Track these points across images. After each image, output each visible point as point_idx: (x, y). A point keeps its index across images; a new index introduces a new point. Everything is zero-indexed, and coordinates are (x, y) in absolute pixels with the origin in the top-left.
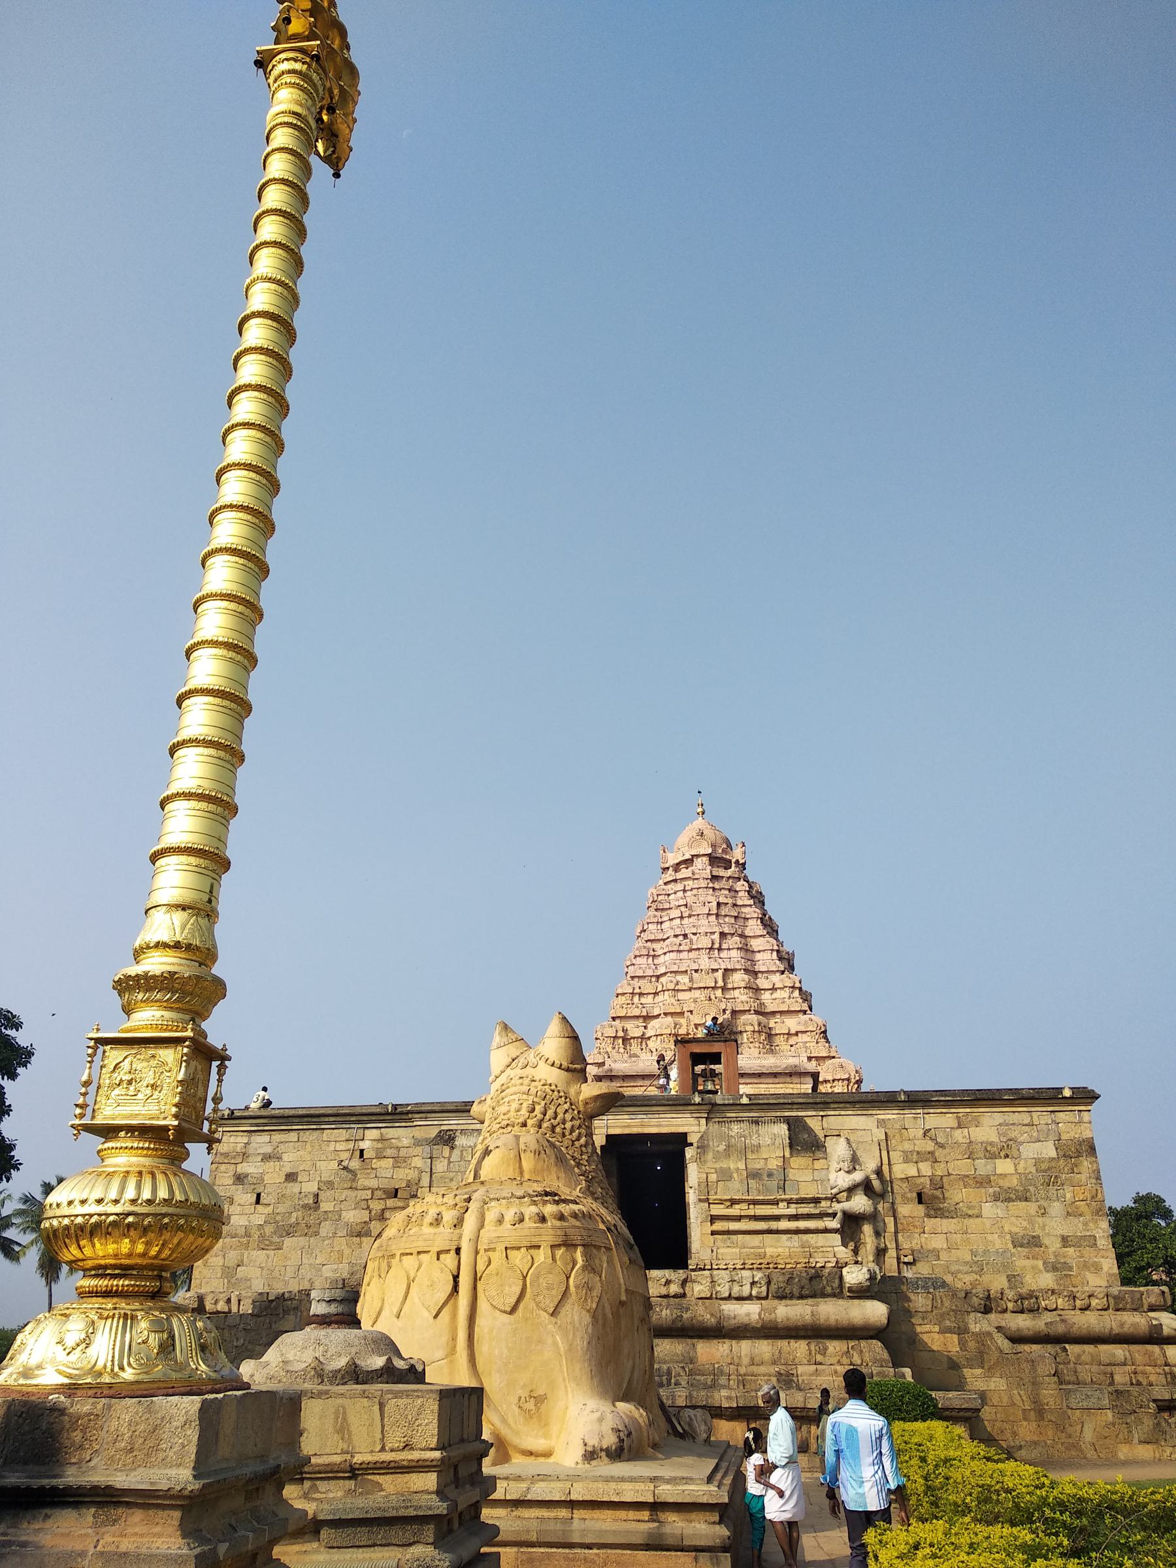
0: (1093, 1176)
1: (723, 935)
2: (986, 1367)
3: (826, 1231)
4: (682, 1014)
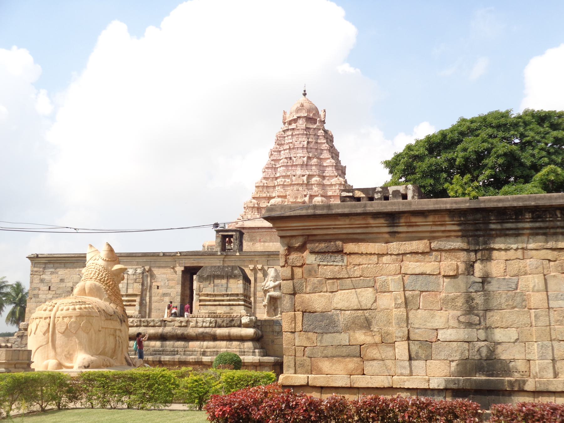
3: (239, 305)
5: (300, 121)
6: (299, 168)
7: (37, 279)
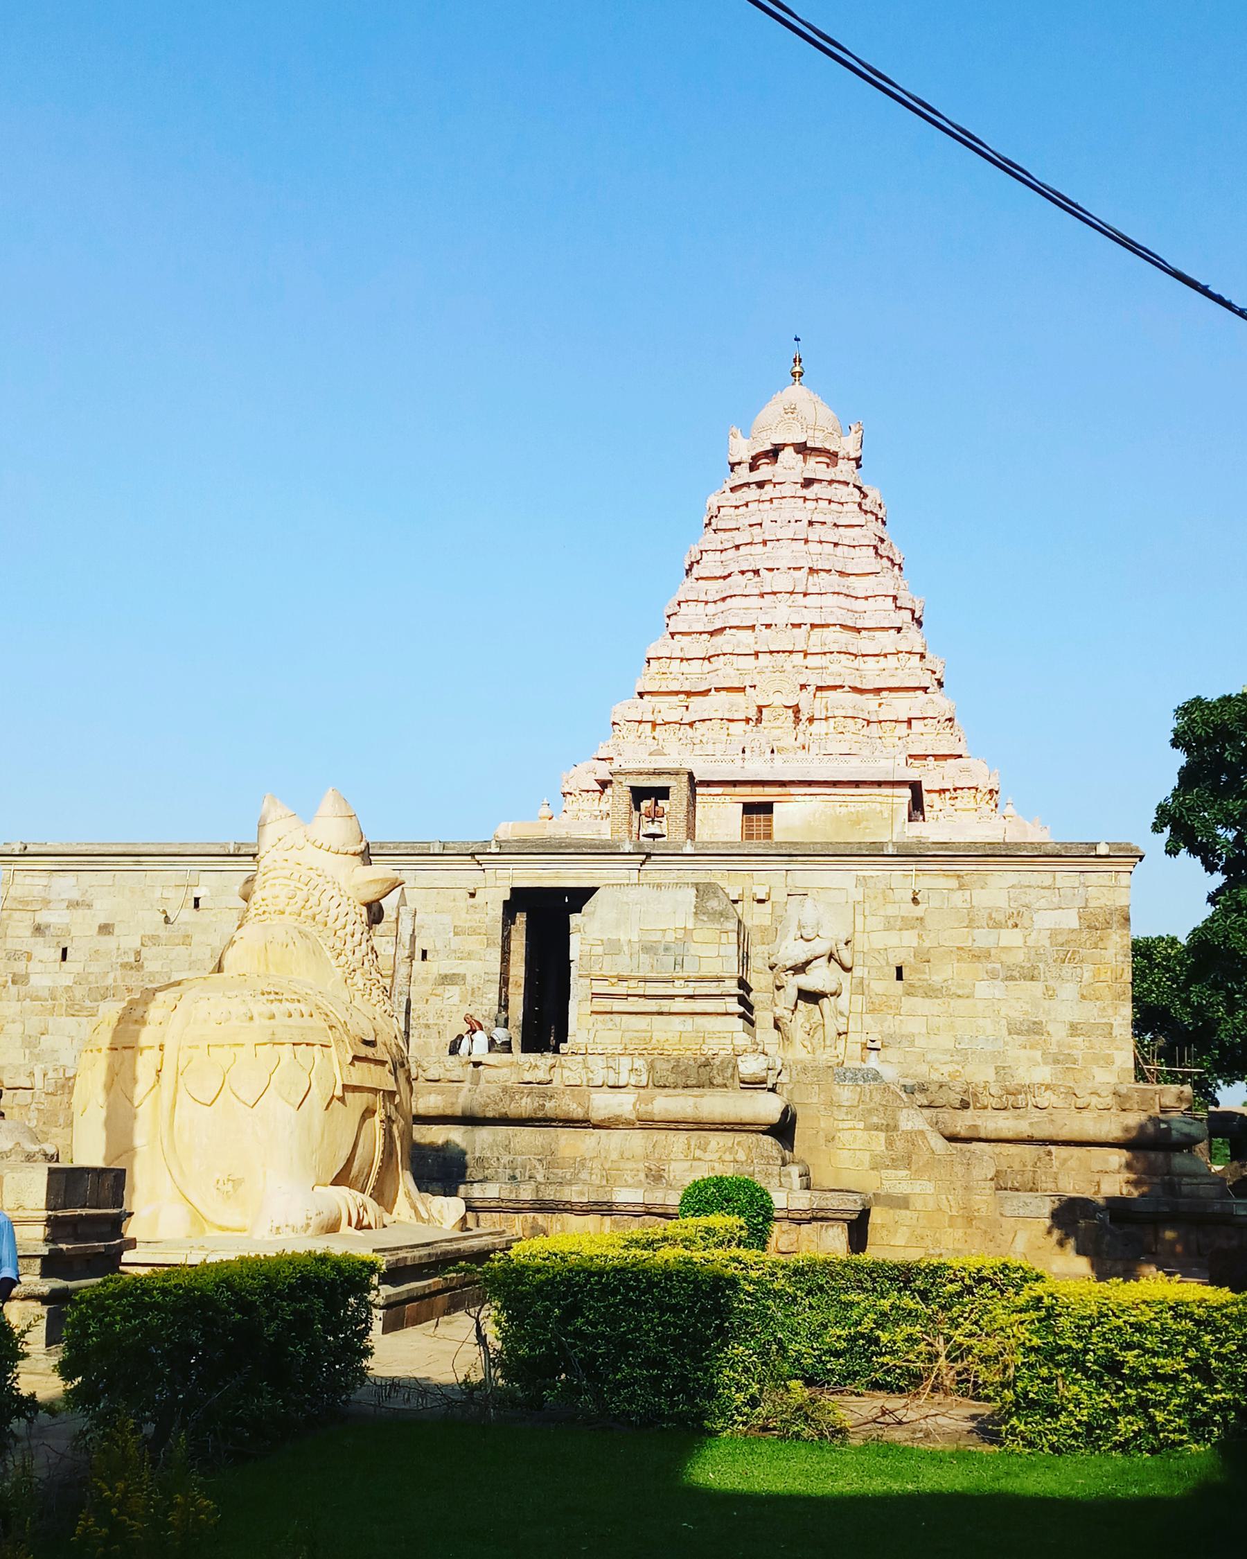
0: (1121, 952)
2: (914, 1168)
5: (787, 455)
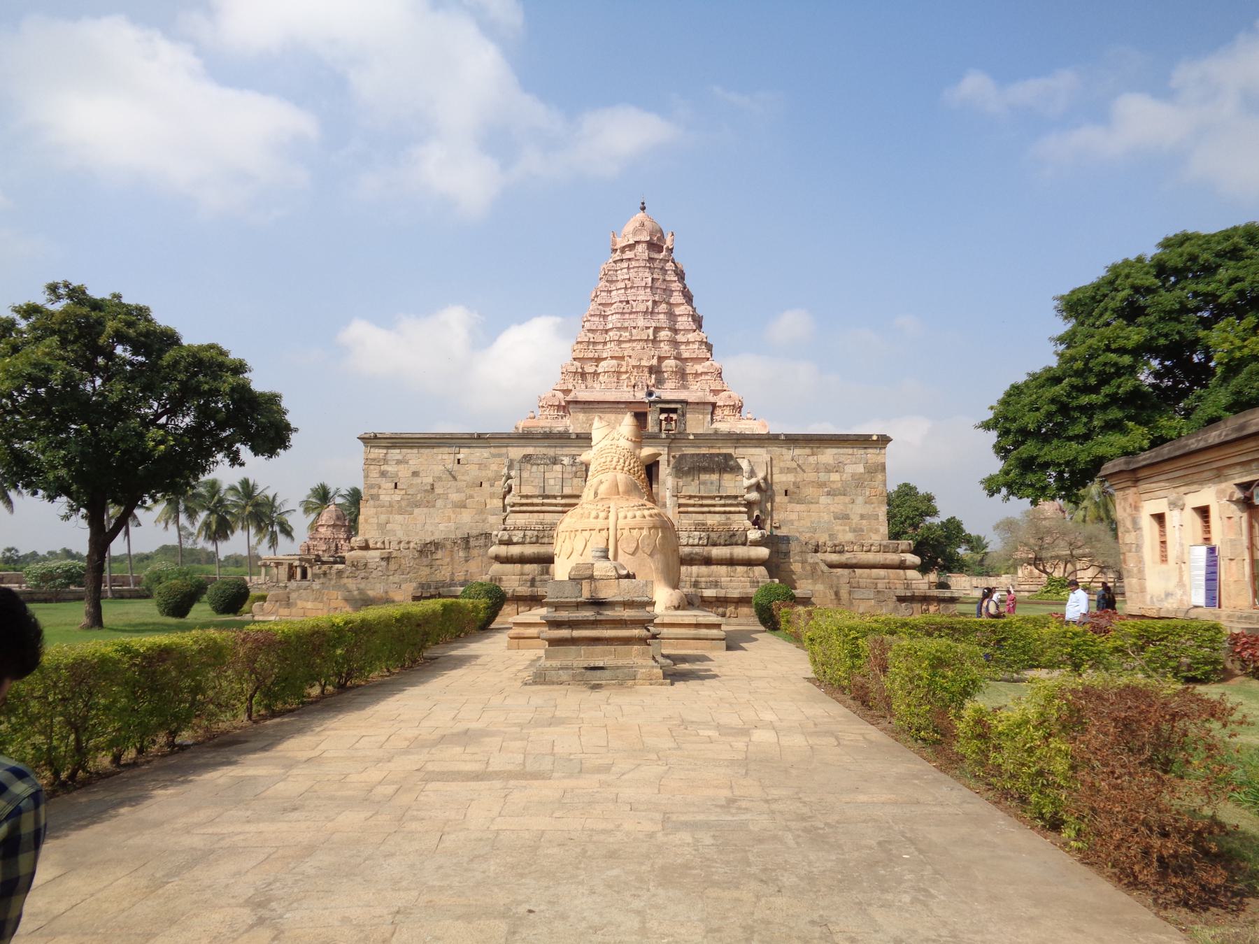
1: (655, 302)
3: (740, 512)
4: (622, 358)
5: (641, 248)
6: (641, 317)
7: (374, 473)
